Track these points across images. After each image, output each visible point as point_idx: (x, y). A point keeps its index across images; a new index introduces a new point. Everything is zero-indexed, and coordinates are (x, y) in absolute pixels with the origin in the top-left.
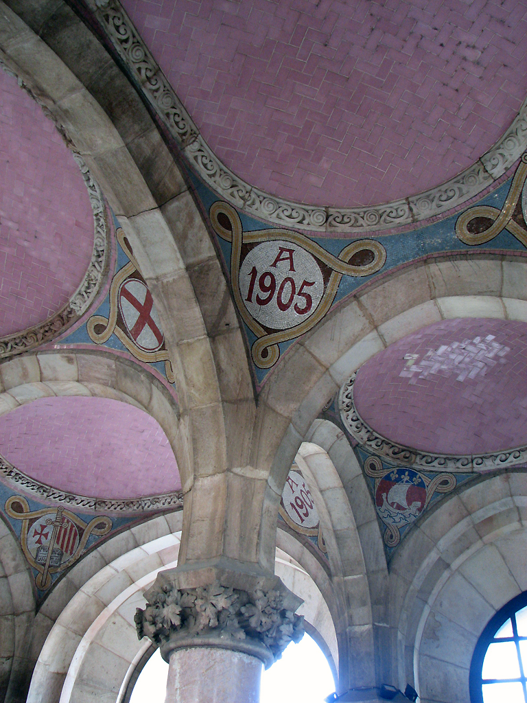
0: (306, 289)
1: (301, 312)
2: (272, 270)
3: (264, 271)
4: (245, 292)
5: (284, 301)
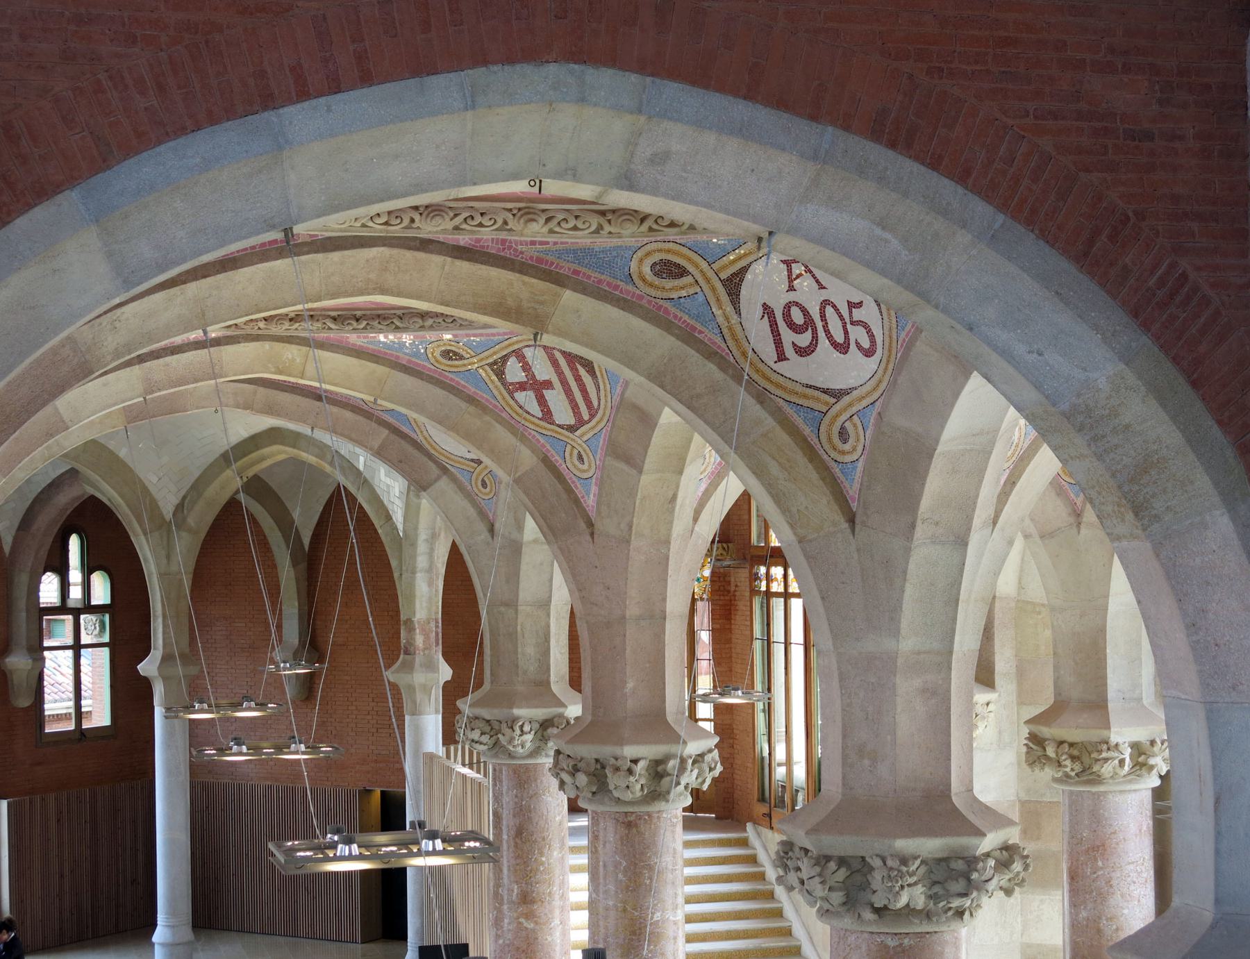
0: (858, 314)
1: (869, 353)
2: (792, 296)
3: (783, 302)
4: (769, 353)
5: (840, 338)
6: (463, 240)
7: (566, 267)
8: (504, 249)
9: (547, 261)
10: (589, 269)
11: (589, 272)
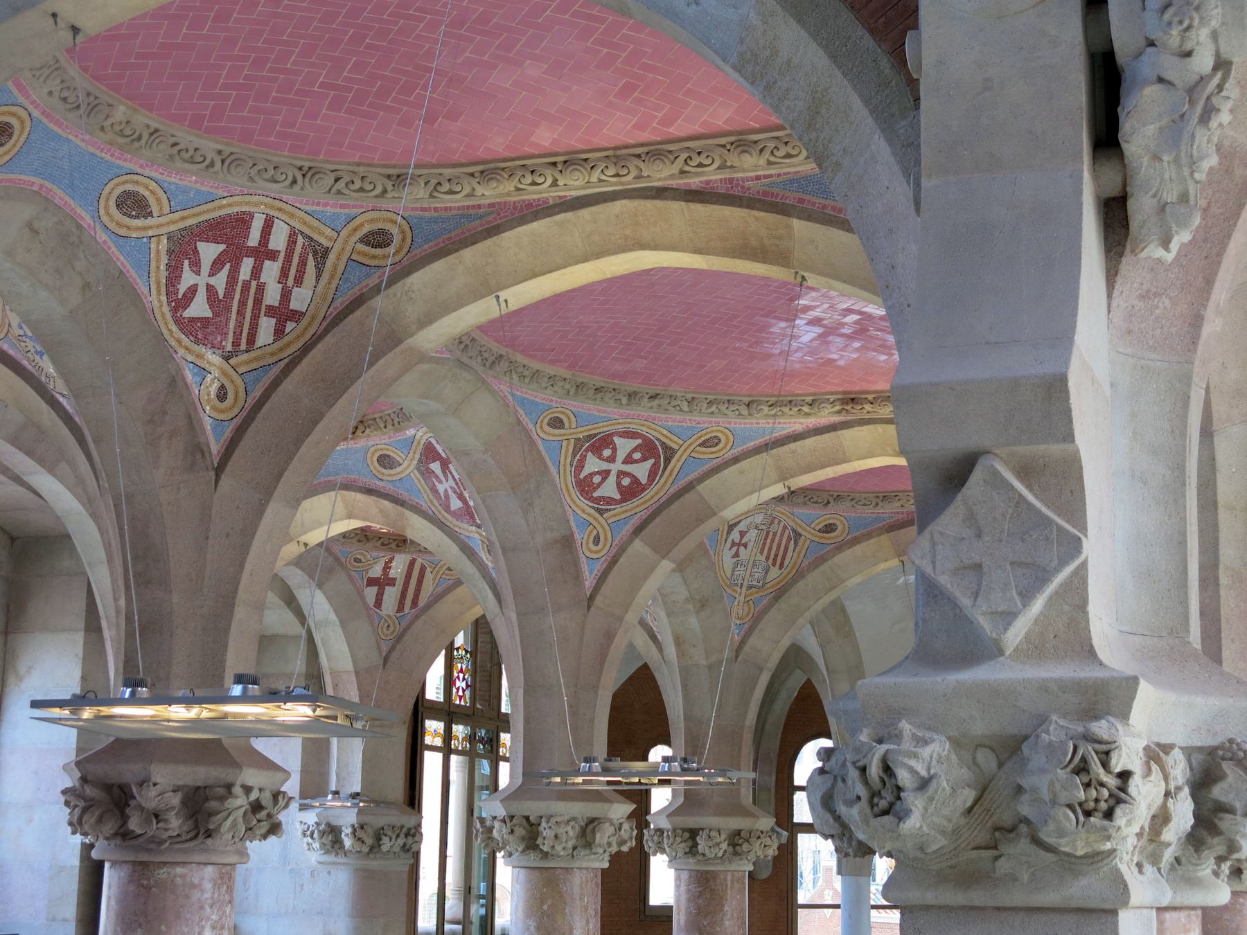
6: (694, 182)
7: (791, 197)
8: (732, 187)
9: (773, 194)
10: (813, 196)
11: (814, 199)
